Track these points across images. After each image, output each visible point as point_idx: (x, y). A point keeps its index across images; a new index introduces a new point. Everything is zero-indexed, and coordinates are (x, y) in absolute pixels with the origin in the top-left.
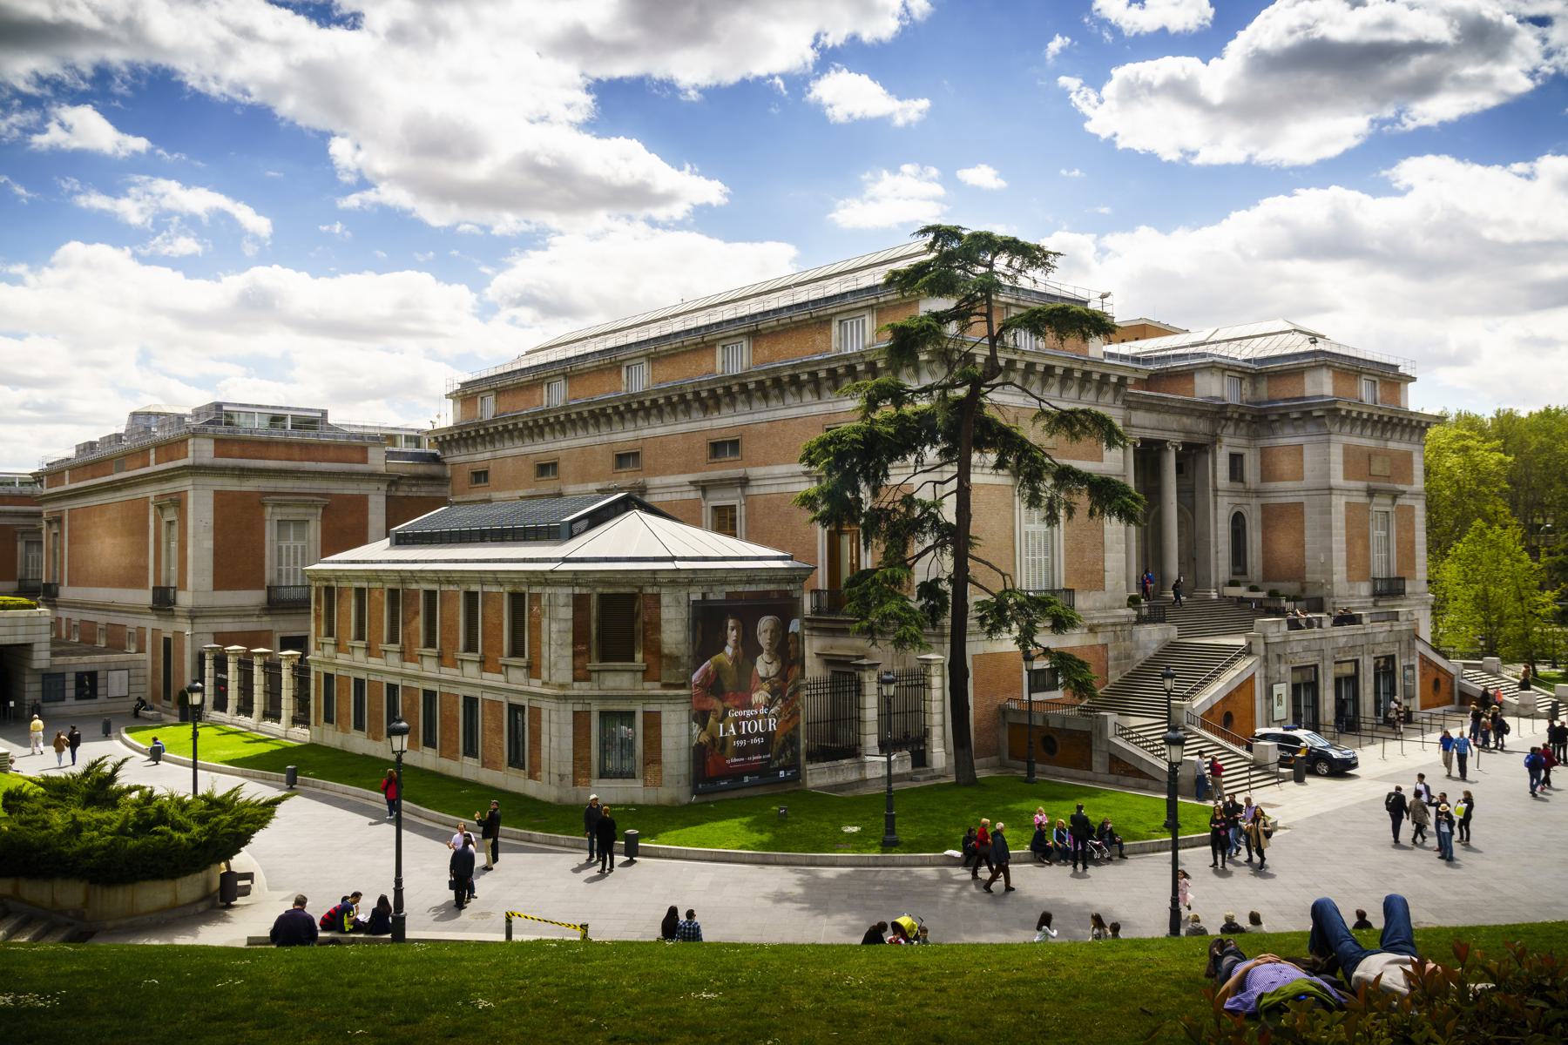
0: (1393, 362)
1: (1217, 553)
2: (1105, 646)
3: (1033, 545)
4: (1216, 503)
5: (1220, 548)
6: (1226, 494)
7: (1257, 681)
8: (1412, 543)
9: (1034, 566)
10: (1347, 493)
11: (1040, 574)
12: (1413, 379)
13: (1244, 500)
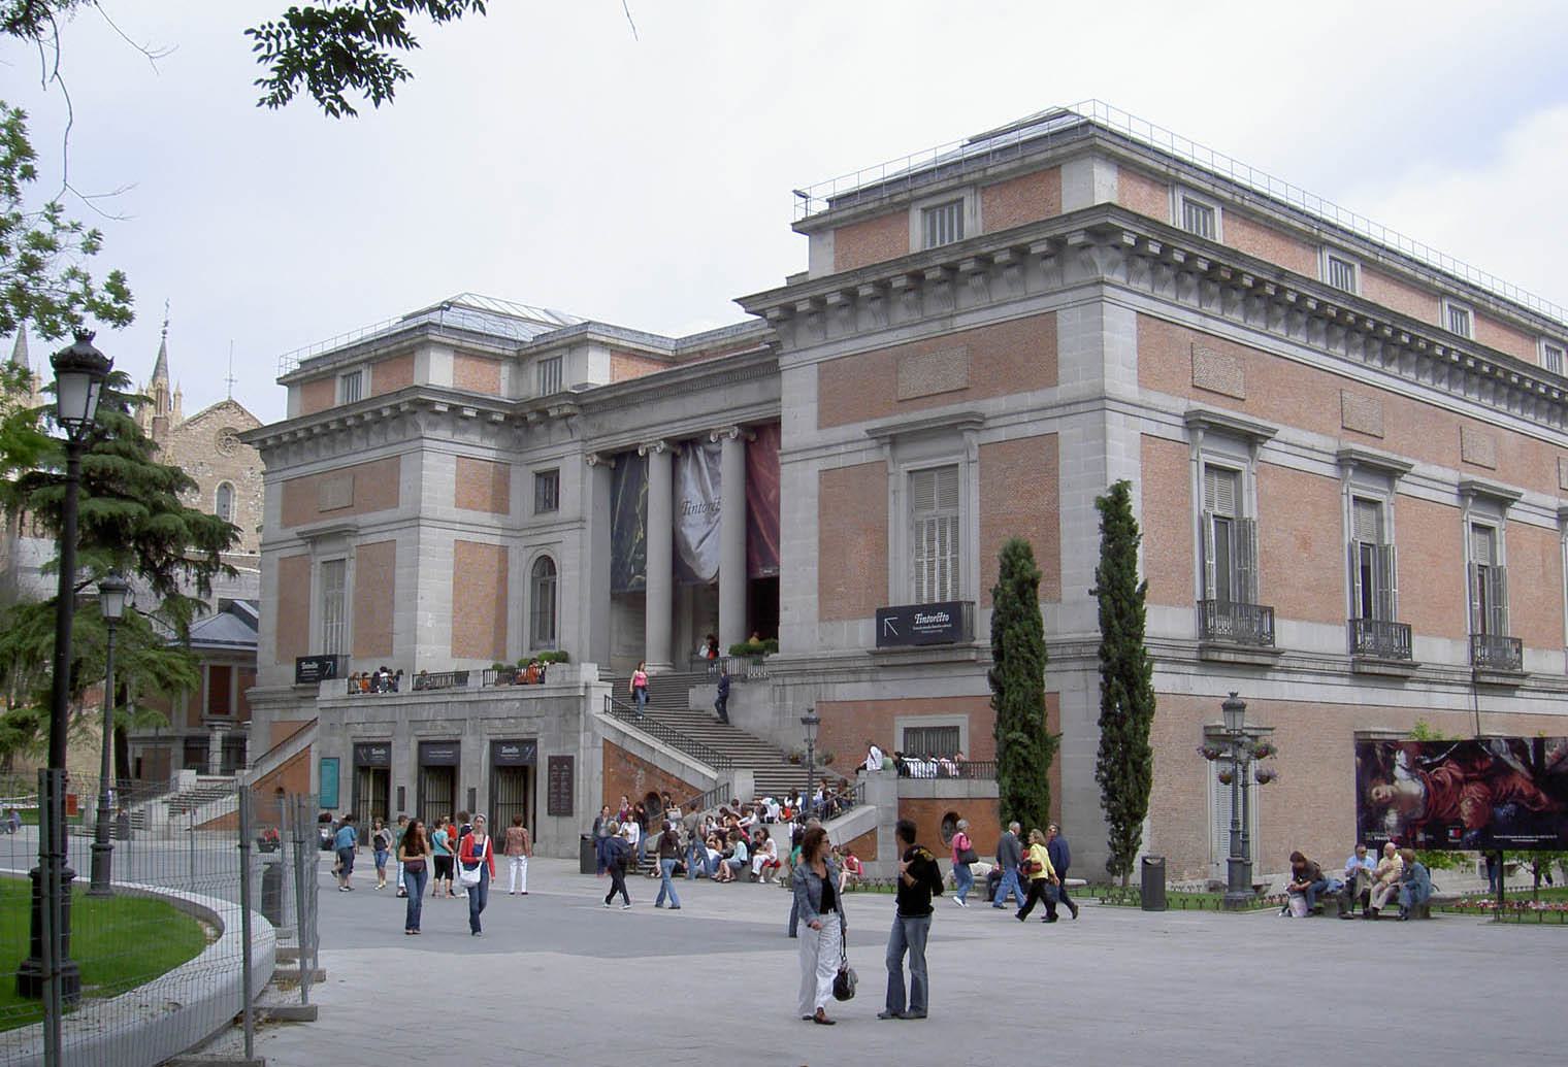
10: (824, 452)
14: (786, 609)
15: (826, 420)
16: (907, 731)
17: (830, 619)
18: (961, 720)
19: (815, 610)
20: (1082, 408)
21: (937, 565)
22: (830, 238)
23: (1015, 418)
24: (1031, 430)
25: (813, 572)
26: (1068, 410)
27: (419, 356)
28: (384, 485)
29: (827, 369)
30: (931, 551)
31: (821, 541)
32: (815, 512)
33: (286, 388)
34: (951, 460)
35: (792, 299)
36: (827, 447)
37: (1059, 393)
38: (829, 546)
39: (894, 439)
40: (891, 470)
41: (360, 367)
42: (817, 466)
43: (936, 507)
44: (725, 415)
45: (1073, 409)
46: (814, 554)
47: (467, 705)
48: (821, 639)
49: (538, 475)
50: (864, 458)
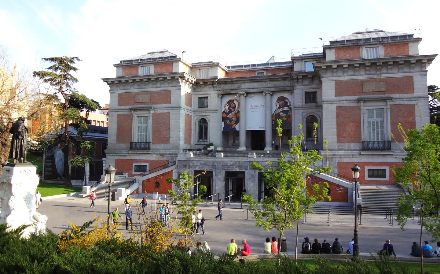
3: (141, 130)
6: (301, 108)
9: (141, 136)
10: (338, 102)
11: (143, 138)
13: (316, 110)
15: (338, 94)
16: (368, 170)
17: (341, 143)
18: (387, 168)
19: (336, 140)
20: (422, 99)
21: (376, 131)
22: (333, 51)
23: (402, 99)
24: (406, 103)
25: (335, 131)
26: (418, 99)
27: (174, 64)
28: (166, 97)
29: (337, 83)
30: (374, 128)
31: (337, 123)
32: (335, 116)
33: (116, 68)
34: (381, 107)
35: (332, 64)
36: (339, 101)
37: (415, 95)
38: (340, 126)
39: (365, 101)
40: (362, 108)
41: (150, 65)
42: (335, 106)
44: (268, 88)
45: (420, 99)
46: (336, 126)
47: (248, 162)
48: (338, 147)
49: (199, 98)
50: (352, 105)
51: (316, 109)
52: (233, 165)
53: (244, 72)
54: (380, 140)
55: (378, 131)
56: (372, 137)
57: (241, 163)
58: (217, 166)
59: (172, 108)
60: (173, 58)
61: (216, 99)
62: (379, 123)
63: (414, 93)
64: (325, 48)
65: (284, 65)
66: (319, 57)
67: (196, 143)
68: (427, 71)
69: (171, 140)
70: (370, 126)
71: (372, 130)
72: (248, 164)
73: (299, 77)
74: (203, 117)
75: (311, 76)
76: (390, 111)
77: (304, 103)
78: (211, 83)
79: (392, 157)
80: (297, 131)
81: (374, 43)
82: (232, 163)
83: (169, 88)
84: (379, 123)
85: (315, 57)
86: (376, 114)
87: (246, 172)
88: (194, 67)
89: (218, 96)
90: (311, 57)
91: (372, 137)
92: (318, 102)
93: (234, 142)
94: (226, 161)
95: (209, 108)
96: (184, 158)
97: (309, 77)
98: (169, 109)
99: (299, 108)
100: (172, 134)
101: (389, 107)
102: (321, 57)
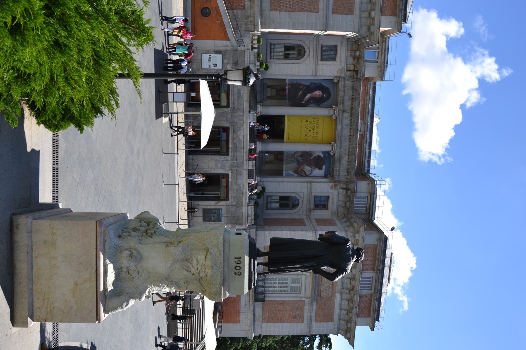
0: (380, 319)
1: (279, 182)
2: (243, 8)
4: (304, 182)
5: (281, 183)
6: (309, 191)
7: (225, 42)
8: (281, 320)
12: (372, 329)
14: (269, 233)
27: (393, 19)
30: (279, 283)
37: (314, 323)
43: (290, 285)
49: (336, 47)
51: (307, 209)
52: (239, 185)
53: (365, 105)
54: (266, 289)
55: (276, 288)
56: (269, 281)
57: (241, 151)
58: (236, 114)
59: (327, 17)
60: (403, 17)
61: (331, 75)
62: (286, 289)
63: (315, 322)
64: (381, 232)
65: (367, 160)
66: (371, 214)
67: (269, 41)
68: (337, 335)
69: (274, 14)
70: (282, 279)
71: (277, 281)
72: (240, 161)
73: (349, 192)
74: (307, 53)
75: (348, 206)
76: (297, 300)
77: (315, 194)
78: (356, 69)
79: (247, 301)
80: (280, 185)
81: (377, 286)
82: (242, 139)
83: (357, 12)
84: (286, 289)
85: (371, 209)
86: (295, 286)
87: (229, 158)
88: (384, 39)
89: (336, 77)
90: (371, 205)
91: (269, 281)
92: (315, 211)
93: (268, 87)
94: (244, 129)
95: (320, 63)
96: (249, 62)
97: (348, 204)
98: (325, 12)
99: (309, 189)
100: (284, 16)
101: (303, 299)
102: (370, 217)
